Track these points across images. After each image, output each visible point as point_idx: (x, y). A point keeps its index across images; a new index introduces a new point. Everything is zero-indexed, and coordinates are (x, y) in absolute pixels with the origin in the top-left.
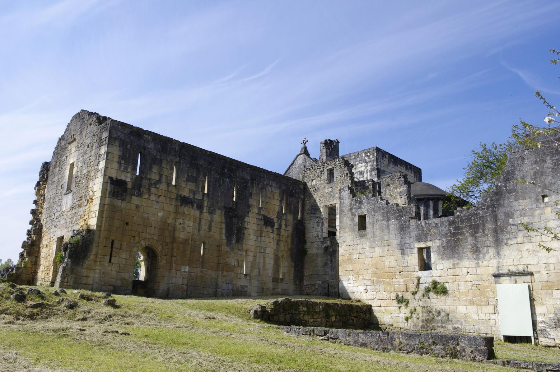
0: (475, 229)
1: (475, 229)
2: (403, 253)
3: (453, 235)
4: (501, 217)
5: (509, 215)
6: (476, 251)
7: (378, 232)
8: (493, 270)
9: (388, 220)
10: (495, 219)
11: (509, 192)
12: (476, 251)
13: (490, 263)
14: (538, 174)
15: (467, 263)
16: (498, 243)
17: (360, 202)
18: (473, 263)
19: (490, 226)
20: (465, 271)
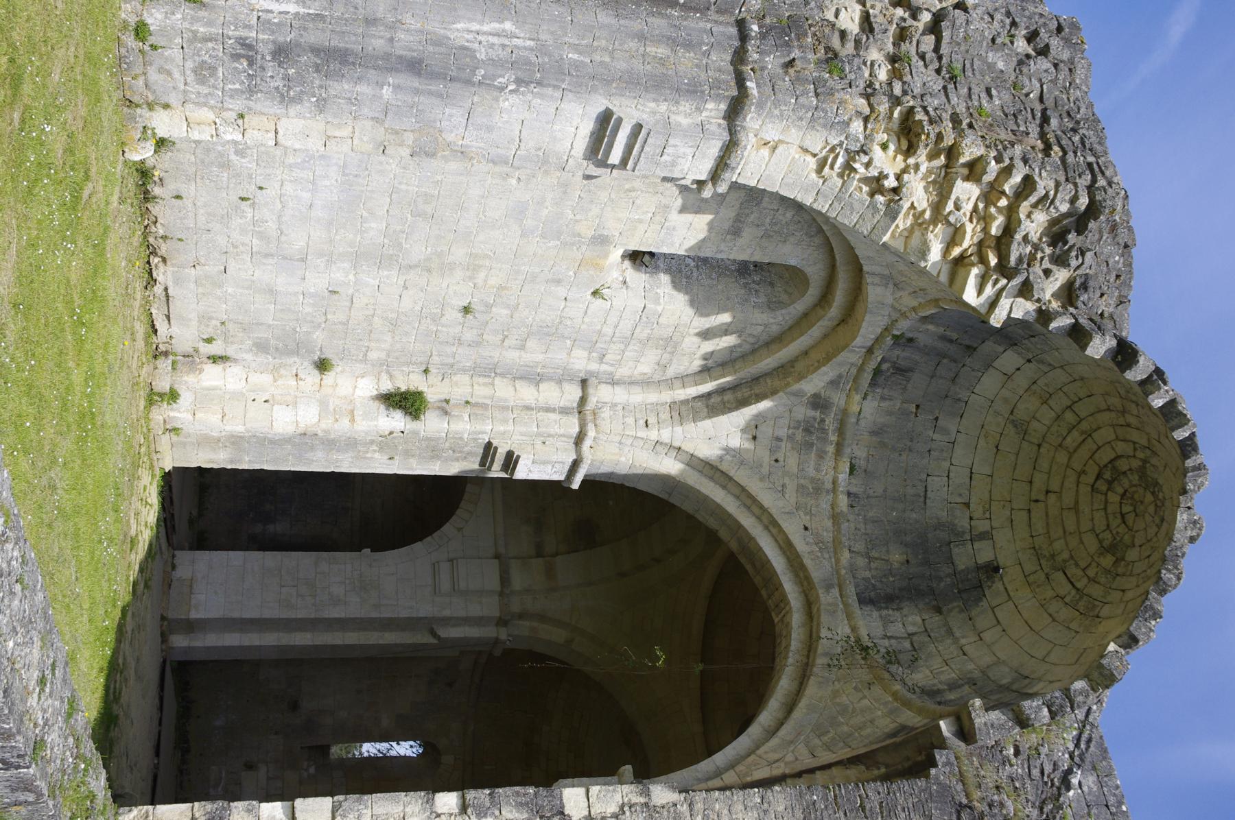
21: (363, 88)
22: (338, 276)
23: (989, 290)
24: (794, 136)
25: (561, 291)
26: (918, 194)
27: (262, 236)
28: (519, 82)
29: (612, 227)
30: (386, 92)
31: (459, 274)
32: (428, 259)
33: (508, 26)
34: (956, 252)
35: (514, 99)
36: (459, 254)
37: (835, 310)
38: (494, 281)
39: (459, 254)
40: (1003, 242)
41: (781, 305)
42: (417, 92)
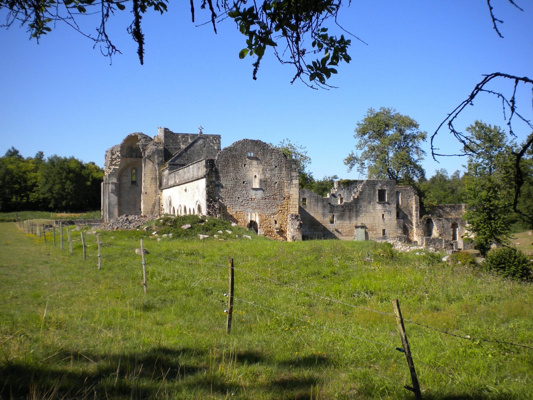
0: (350, 210)
1: (350, 210)
2: (324, 217)
3: (343, 211)
4: (358, 207)
5: (360, 207)
6: (350, 218)
7: (312, 207)
8: (354, 225)
9: (318, 202)
10: (356, 207)
11: (361, 199)
12: (350, 218)
13: (354, 222)
14: (370, 194)
15: (347, 223)
16: (357, 216)
17: (304, 192)
18: (348, 222)
19: (355, 210)
20: (346, 225)
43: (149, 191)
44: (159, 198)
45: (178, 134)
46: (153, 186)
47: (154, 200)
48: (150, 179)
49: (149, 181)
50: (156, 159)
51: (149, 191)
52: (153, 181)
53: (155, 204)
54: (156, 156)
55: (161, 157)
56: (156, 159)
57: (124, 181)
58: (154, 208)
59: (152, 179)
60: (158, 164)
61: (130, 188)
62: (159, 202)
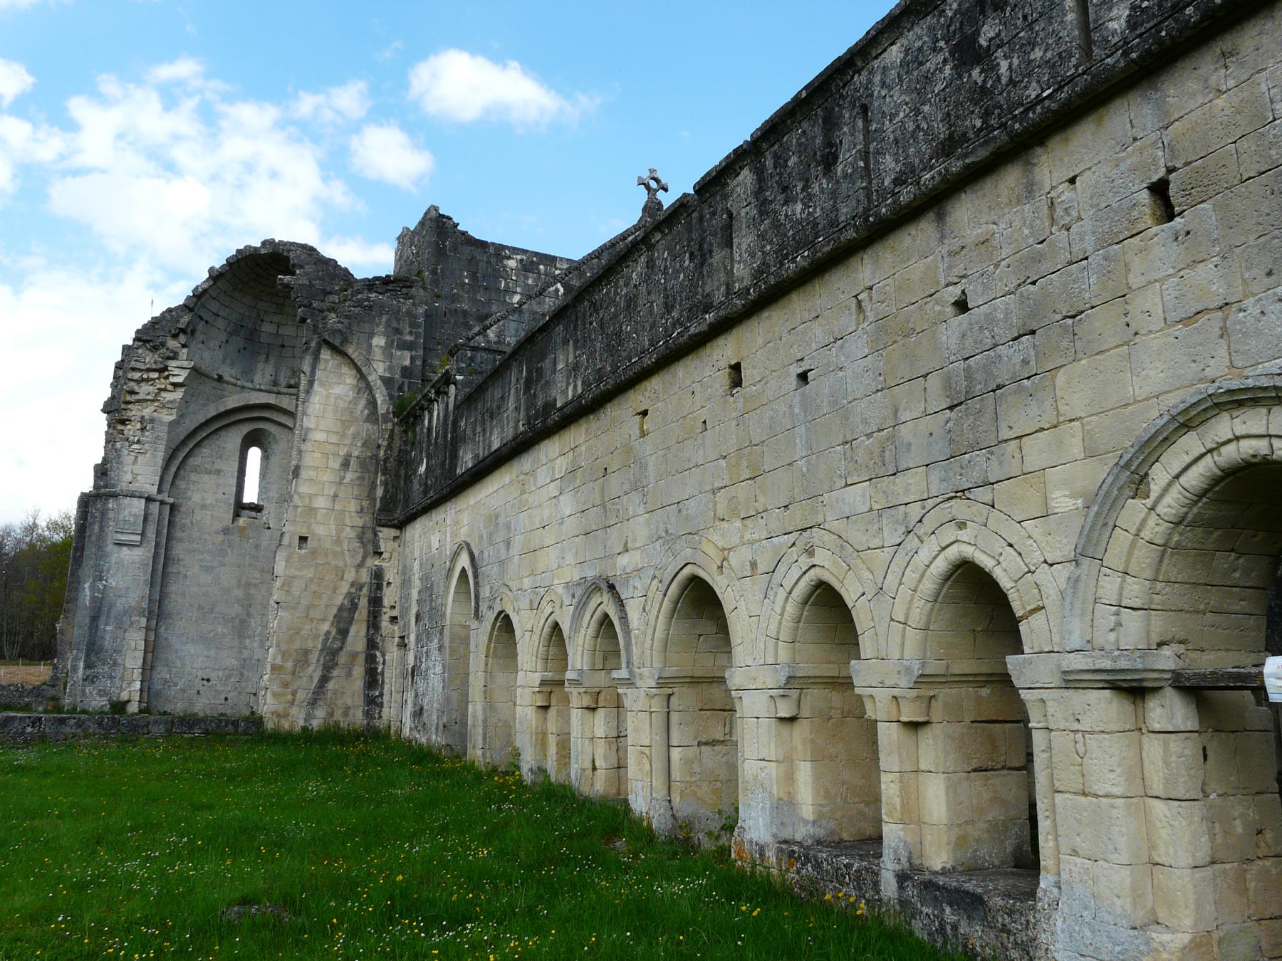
21: (108, 637)
22: (256, 645)
23: (177, 372)
24: (128, 468)
25: (265, 544)
26: (148, 411)
27: (229, 677)
28: (101, 580)
29: (218, 526)
30: (108, 628)
31: (252, 591)
32: (243, 606)
33: (86, 586)
34: (170, 387)
35: (110, 581)
36: (239, 593)
37: (266, 414)
38: (258, 575)
39: (239, 593)
40: (161, 371)
41: (275, 438)
42: (108, 616)
43: (320, 530)
44: (378, 575)
45: (499, 252)
46: (353, 506)
47: (345, 588)
48: (336, 464)
49: (327, 477)
50: (378, 354)
51: (323, 530)
52: (349, 476)
53: (354, 606)
54: (379, 341)
55: (409, 346)
56: (378, 354)
57: (196, 498)
58: (344, 633)
59: (346, 464)
60: (387, 382)
61: (226, 531)
62: (376, 602)
